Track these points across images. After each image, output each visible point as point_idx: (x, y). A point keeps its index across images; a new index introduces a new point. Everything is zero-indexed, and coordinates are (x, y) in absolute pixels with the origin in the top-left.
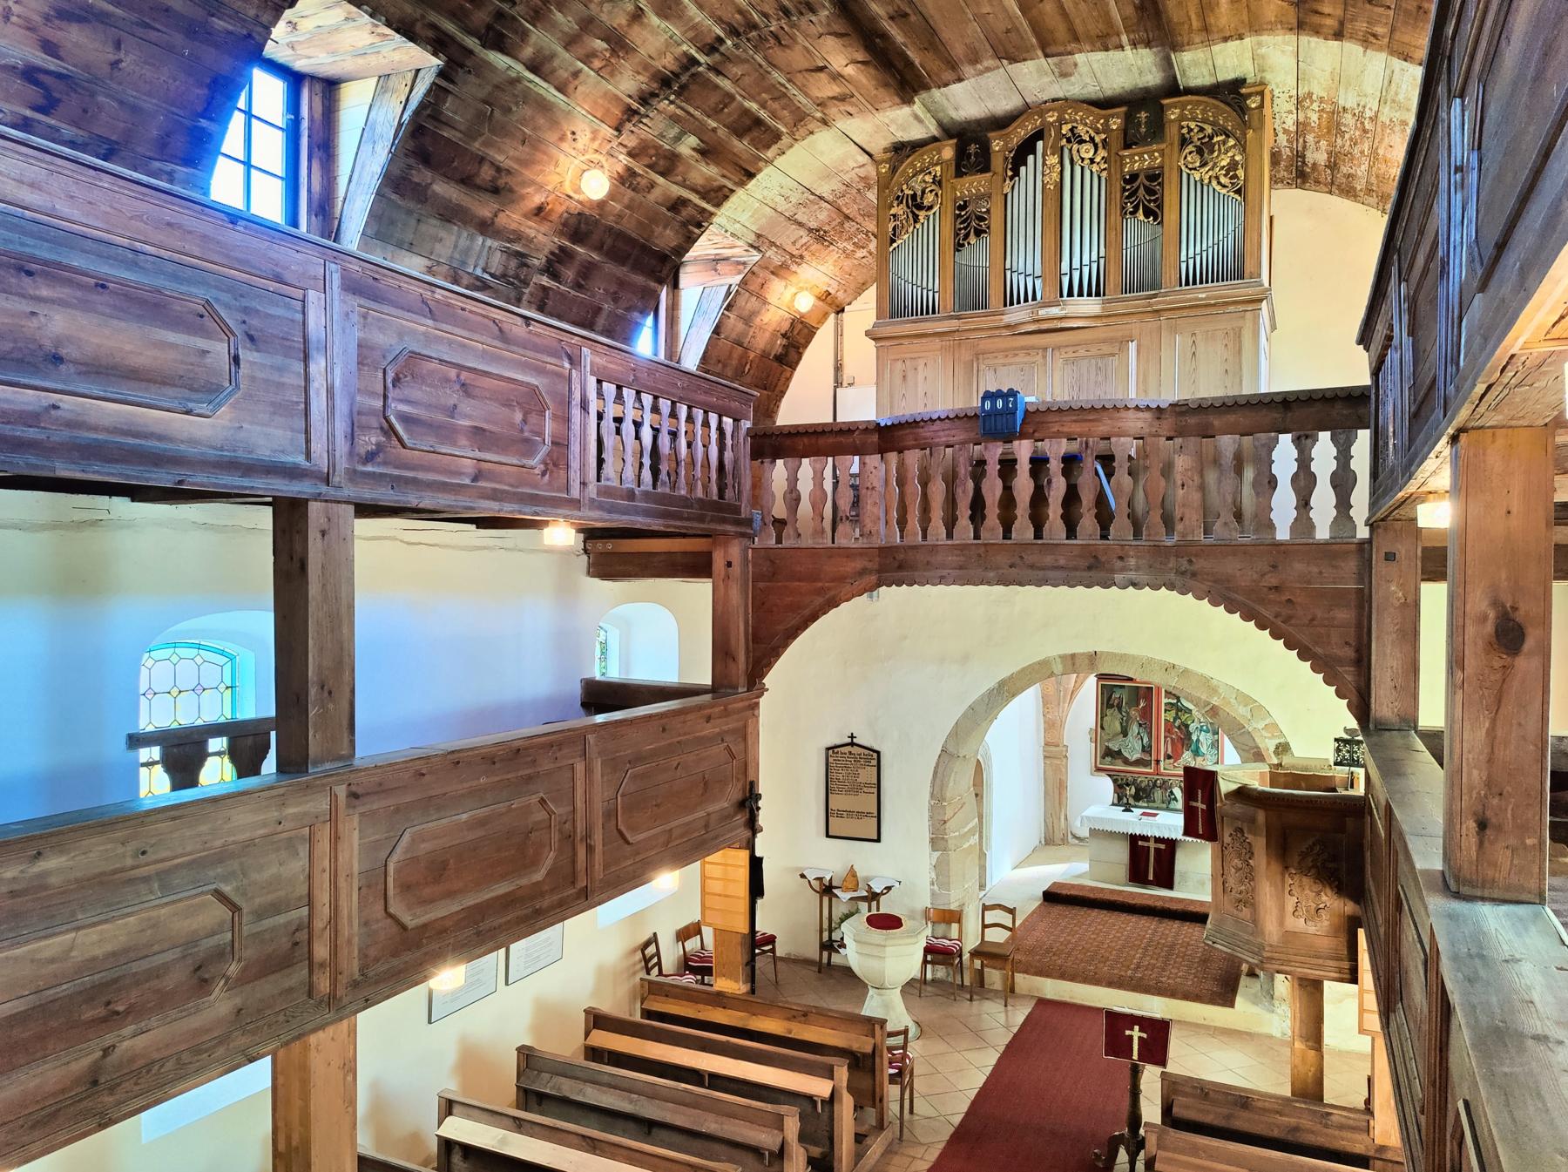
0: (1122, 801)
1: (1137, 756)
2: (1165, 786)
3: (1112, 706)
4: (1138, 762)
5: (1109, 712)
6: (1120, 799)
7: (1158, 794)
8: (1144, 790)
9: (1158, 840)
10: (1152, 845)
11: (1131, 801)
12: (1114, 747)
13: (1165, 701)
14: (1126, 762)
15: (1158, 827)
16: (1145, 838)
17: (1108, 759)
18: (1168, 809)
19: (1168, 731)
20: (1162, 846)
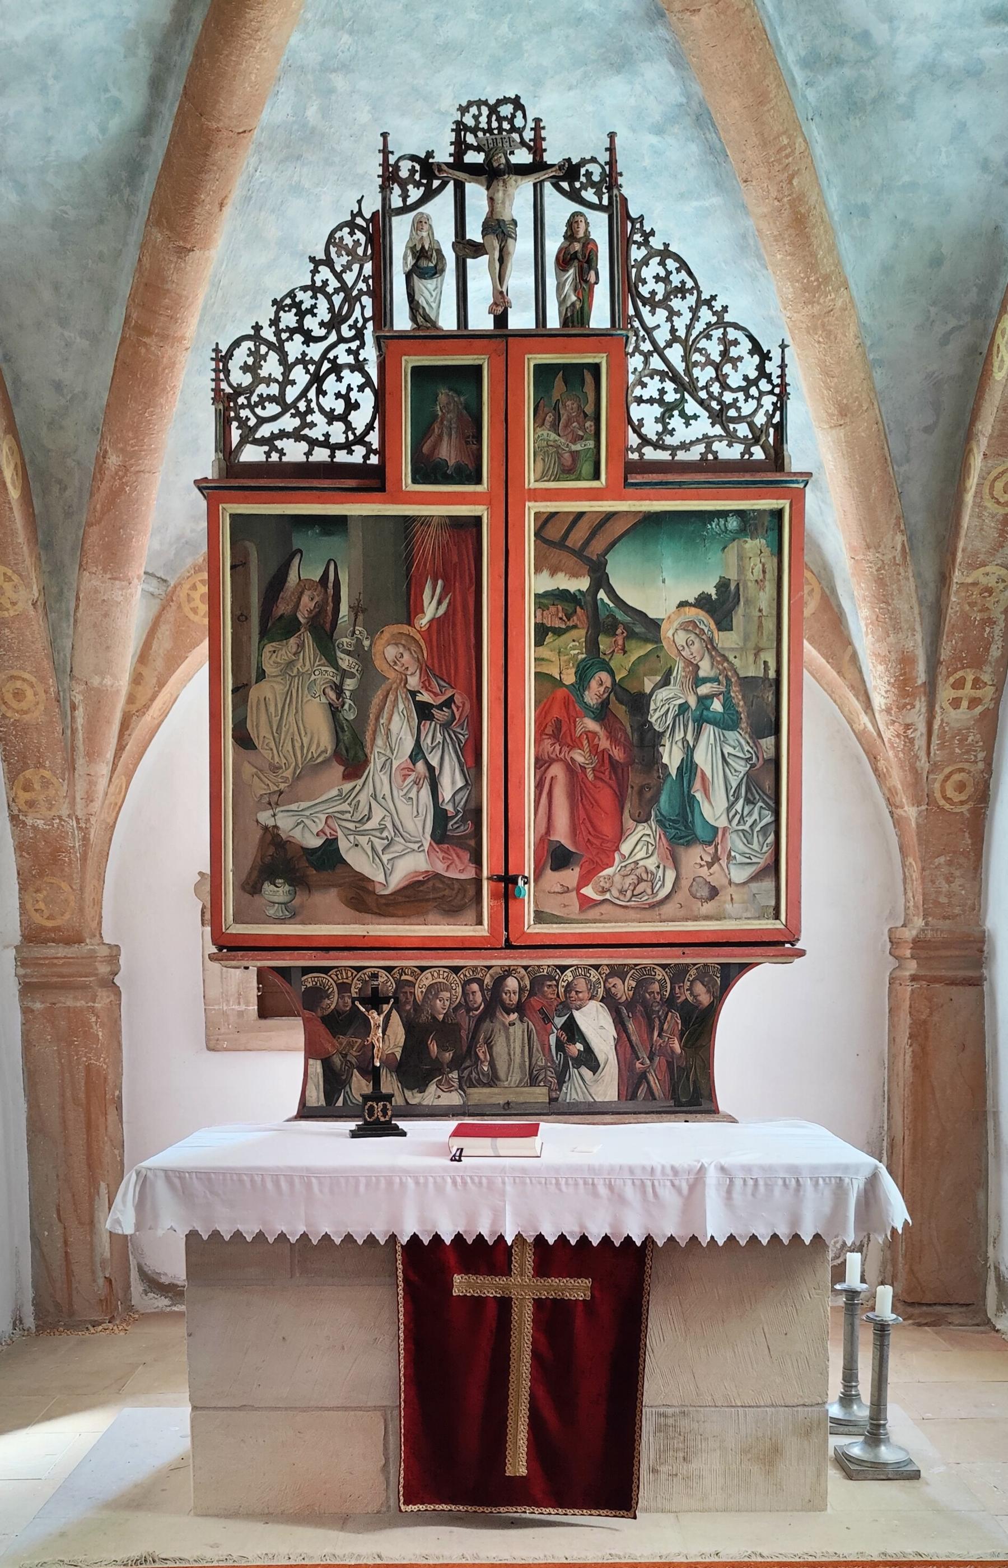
0: (354, 1092)
1: (411, 863)
2: (546, 1004)
3: (289, 627)
4: (418, 897)
5: (274, 657)
6: (334, 1082)
7: (510, 1042)
8: (446, 1030)
9: (554, 1256)
10: (523, 1287)
11: (389, 1084)
12: (303, 827)
13: (537, 583)
14: (362, 897)
15: (556, 1181)
16: (484, 1254)
17: (277, 892)
18: (558, 1109)
19: (555, 729)
20: (577, 1289)
